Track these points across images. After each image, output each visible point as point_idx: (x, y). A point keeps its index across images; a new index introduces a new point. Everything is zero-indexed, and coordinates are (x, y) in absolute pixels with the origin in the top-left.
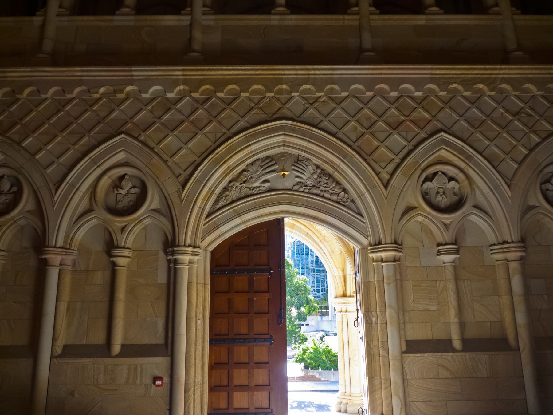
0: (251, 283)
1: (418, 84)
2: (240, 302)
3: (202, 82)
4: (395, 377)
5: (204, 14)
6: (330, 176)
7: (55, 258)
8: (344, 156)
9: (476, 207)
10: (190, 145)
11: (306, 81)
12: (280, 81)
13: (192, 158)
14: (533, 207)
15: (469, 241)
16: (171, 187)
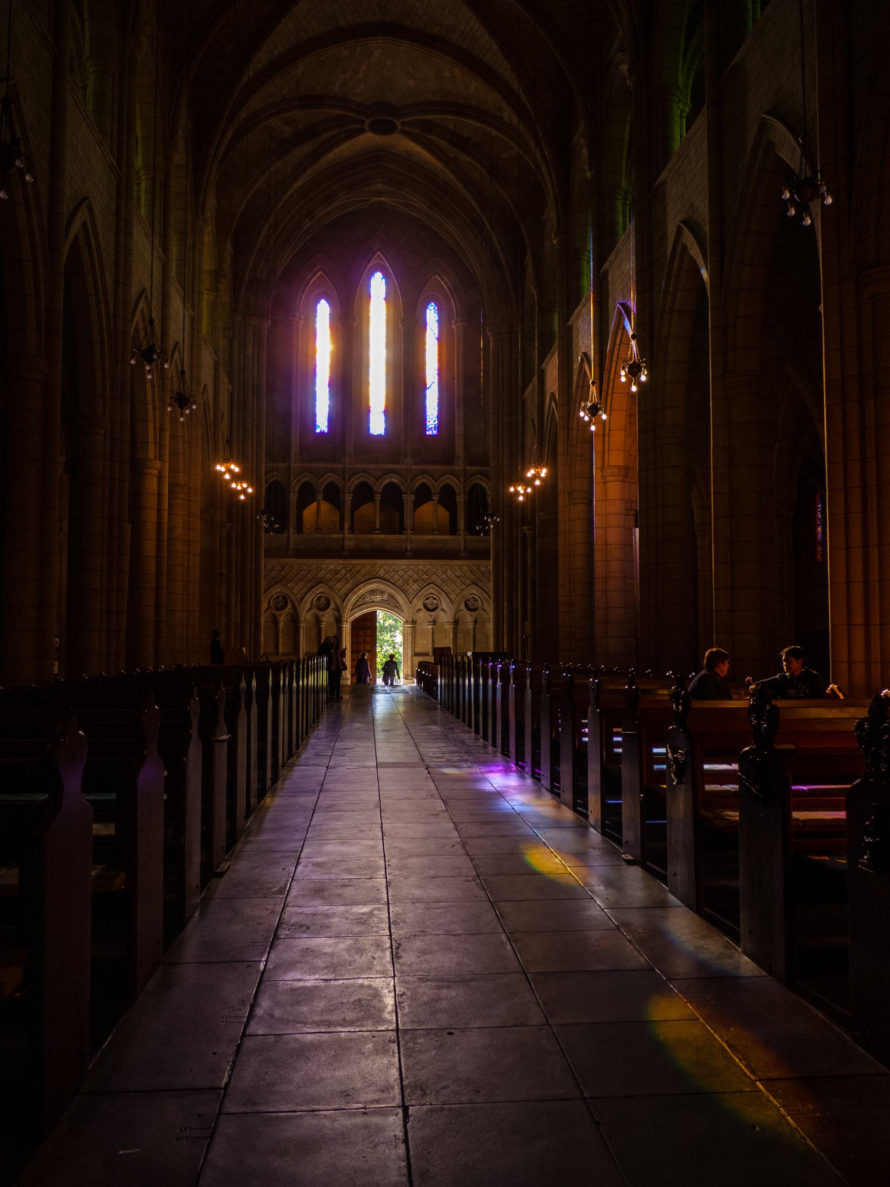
0: (365, 633)
1: (424, 566)
2: (361, 639)
3: (349, 564)
4: (409, 663)
5: (349, 534)
6: (393, 597)
7: (301, 625)
8: (397, 592)
9: (442, 610)
10: (345, 587)
11: (385, 564)
12: (376, 565)
13: (346, 592)
14: (461, 610)
15: (440, 620)
16: (339, 602)
